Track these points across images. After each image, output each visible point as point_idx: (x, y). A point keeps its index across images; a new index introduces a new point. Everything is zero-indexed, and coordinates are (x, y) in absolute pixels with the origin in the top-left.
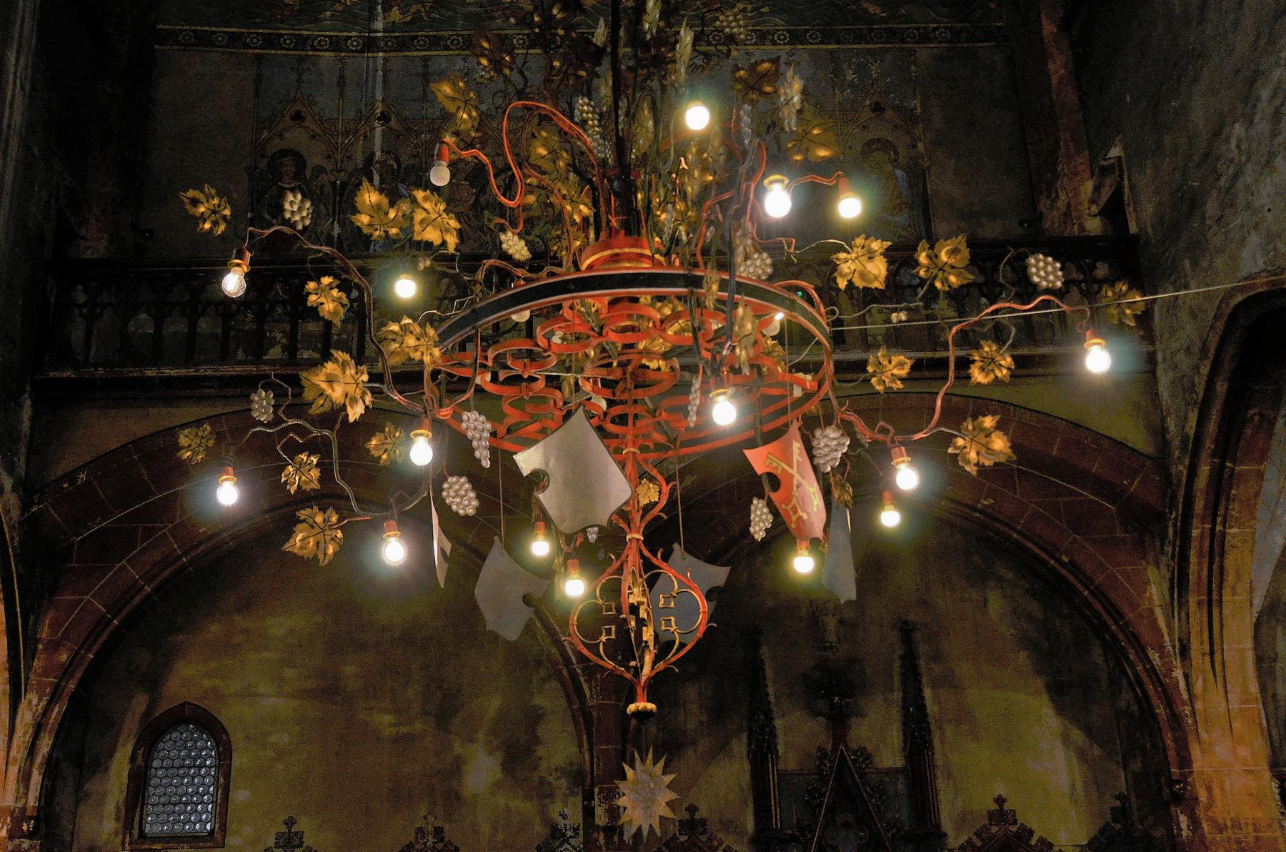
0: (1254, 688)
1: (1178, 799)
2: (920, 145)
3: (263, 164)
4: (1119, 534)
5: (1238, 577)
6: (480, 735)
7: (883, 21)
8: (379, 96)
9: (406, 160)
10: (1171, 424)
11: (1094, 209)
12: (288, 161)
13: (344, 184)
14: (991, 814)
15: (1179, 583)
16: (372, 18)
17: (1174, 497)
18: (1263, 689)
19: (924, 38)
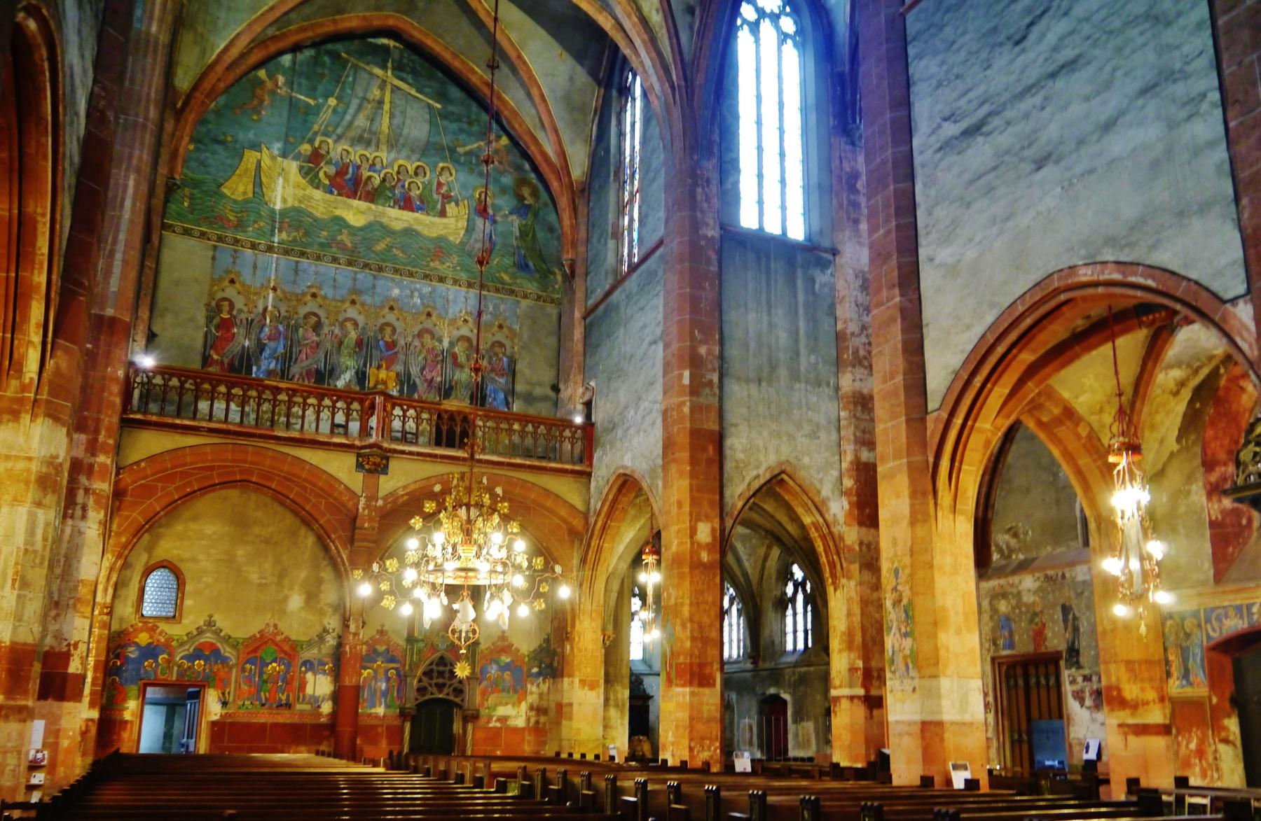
0: (602, 602)
1: (567, 638)
2: (516, 348)
3: (213, 304)
4: (566, 538)
5: (605, 561)
6: (296, 587)
7: (510, 285)
8: (273, 277)
9: (283, 313)
10: (592, 501)
11: (581, 401)
12: (226, 303)
13: (252, 320)
14: (499, 638)
15: (584, 561)
16: (273, 235)
17: (588, 530)
18: (605, 602)
19: (525, 296)
